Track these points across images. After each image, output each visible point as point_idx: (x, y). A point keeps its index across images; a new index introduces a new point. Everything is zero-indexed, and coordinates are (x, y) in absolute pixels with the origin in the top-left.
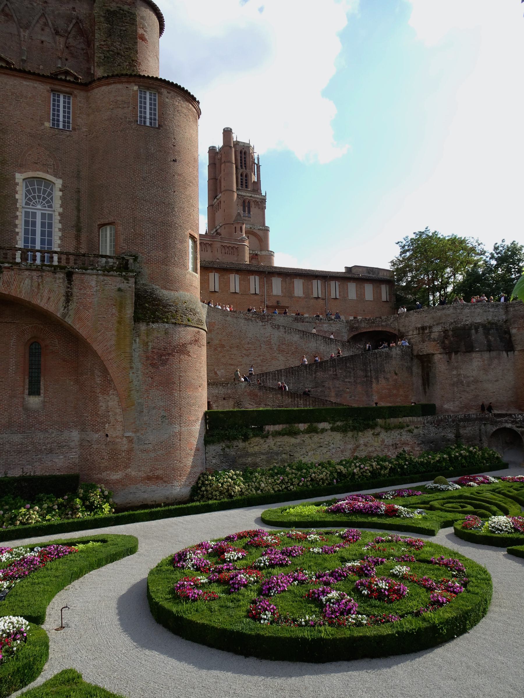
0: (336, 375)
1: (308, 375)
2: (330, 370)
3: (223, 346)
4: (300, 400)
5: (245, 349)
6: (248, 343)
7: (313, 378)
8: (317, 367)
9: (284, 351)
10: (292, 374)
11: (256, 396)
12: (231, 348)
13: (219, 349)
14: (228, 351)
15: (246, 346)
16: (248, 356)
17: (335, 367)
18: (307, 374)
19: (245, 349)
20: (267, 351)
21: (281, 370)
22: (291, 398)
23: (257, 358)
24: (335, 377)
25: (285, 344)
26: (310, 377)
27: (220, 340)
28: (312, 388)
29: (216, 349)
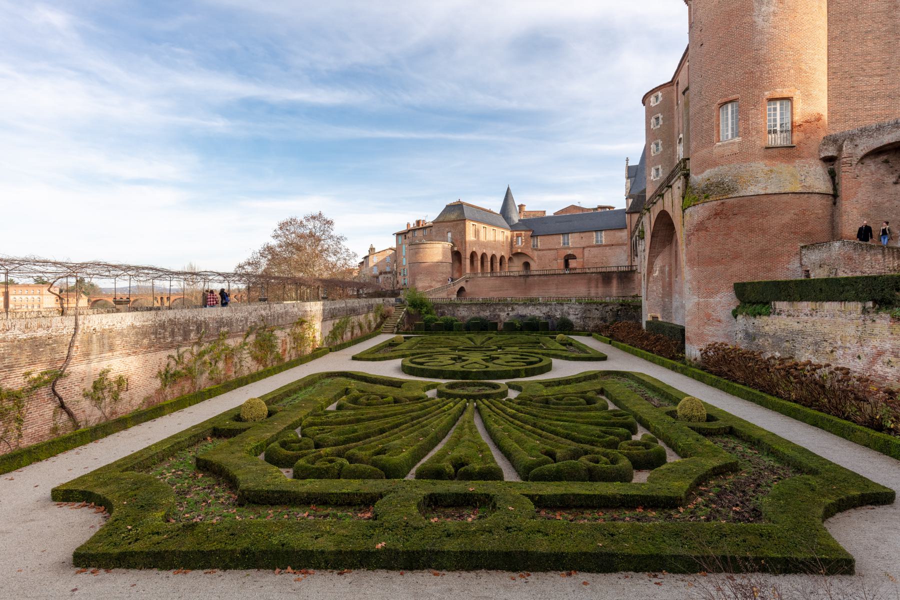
11: (851, 259)
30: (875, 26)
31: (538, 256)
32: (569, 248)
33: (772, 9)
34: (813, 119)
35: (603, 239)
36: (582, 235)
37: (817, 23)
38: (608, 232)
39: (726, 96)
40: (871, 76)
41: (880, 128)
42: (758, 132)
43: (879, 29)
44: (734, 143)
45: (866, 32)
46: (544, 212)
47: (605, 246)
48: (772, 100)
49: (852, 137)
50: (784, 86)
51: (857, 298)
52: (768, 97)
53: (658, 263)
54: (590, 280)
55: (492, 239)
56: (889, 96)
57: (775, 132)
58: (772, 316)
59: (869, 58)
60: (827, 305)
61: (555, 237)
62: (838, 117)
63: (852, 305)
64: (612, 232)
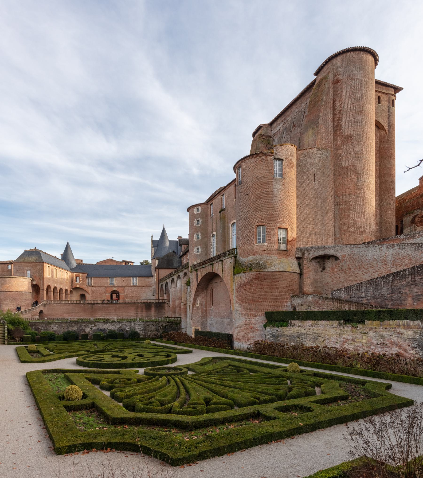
0: (415, 281)
1: (385, 284)
2: (408, 277)
3: (350, 269)
4: (346, 305)
5: (365, 269)
6: (368, 264)
7: (390, 286)
8: (394, 276)
9: (398, 265)
10: (371, 285)
11: (318, 303)
12: (355, 269)
13: (347, 272)
14: (353, 272)
15: (365, 267)
16: (367, 273)
17: (414, 274)
18: (384, 283)
19: (365, 269)
20: (382, 267)
21: (361, 283)
22: (340, 303)
23: (374, 274)
24: (414, 283)
25: (399, 258)
26: (387, 285)
27: (348, 266)
28: (388, 294)
29: (345, 272)
31: (92, 290)
32: (114, 287)
35: (138, 282)
36: (124, 279)
38: (141, 278)
39: (260, 222)
40: (309, 224)
41: (318, 248)
46: (82, 260)
47: (138, 286)
48: (280, 228)
49: (308, 250)
51: (336, 319)
53: (199, 300)
54: (137, 308)
55: (60, 277)
57: (281, 243)
58: (289, 327)
60: (321, 322)
61: (104, 279)
63: (333, 322)
64: (143, 279)
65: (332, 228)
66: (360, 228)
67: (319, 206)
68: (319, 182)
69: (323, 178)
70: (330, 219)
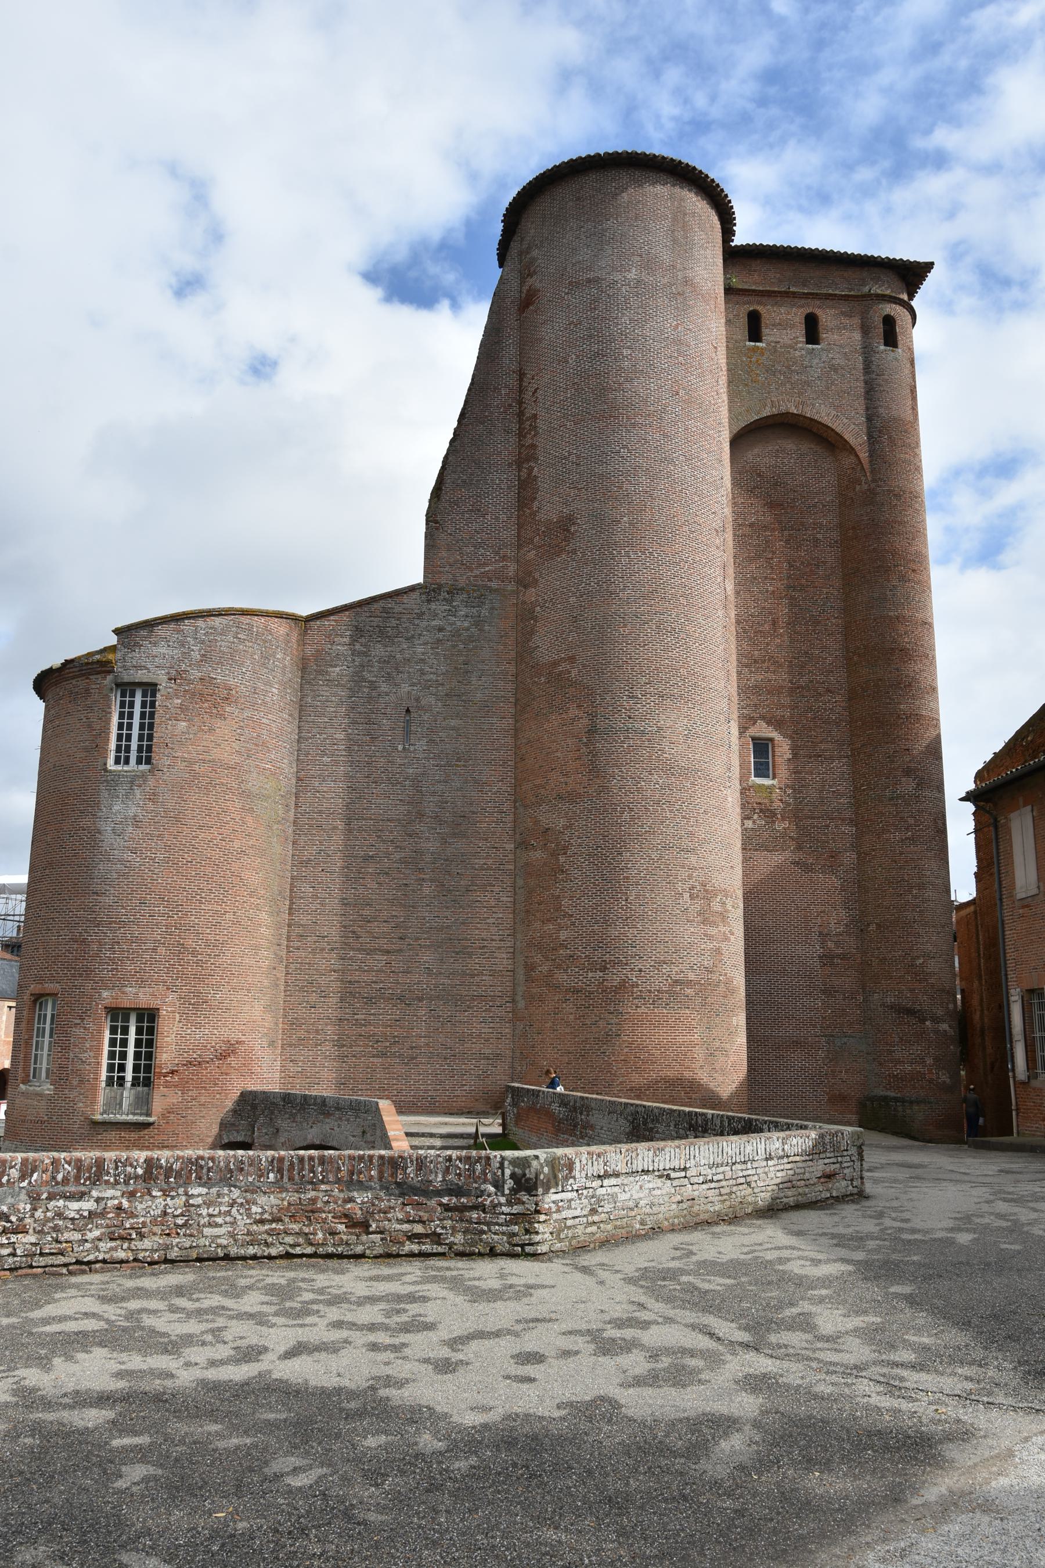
30: (382, 847)
33: (132, 811)
34: (209, 1055)
37: (237, 844)
42: (81, 1082)
43: (388, 855)
44: (40, 1095)
45: (367, 858)
50: (142, 983)
52: (107, 1002)
56: (401, 998)
59: (366, 912)
62: (302, 1034)
65: (503, 960)
66: (604, 969)
67: (428, 858)
68: (431, 741)
69: (453, 723)
70: (491, 916)
